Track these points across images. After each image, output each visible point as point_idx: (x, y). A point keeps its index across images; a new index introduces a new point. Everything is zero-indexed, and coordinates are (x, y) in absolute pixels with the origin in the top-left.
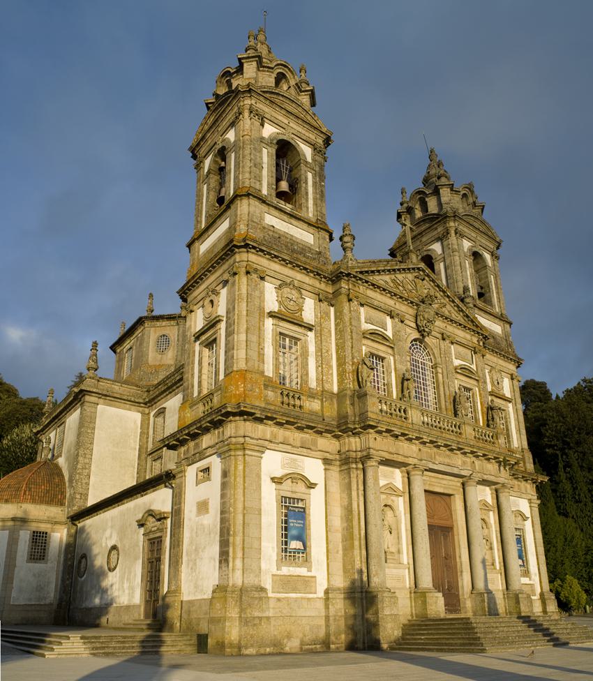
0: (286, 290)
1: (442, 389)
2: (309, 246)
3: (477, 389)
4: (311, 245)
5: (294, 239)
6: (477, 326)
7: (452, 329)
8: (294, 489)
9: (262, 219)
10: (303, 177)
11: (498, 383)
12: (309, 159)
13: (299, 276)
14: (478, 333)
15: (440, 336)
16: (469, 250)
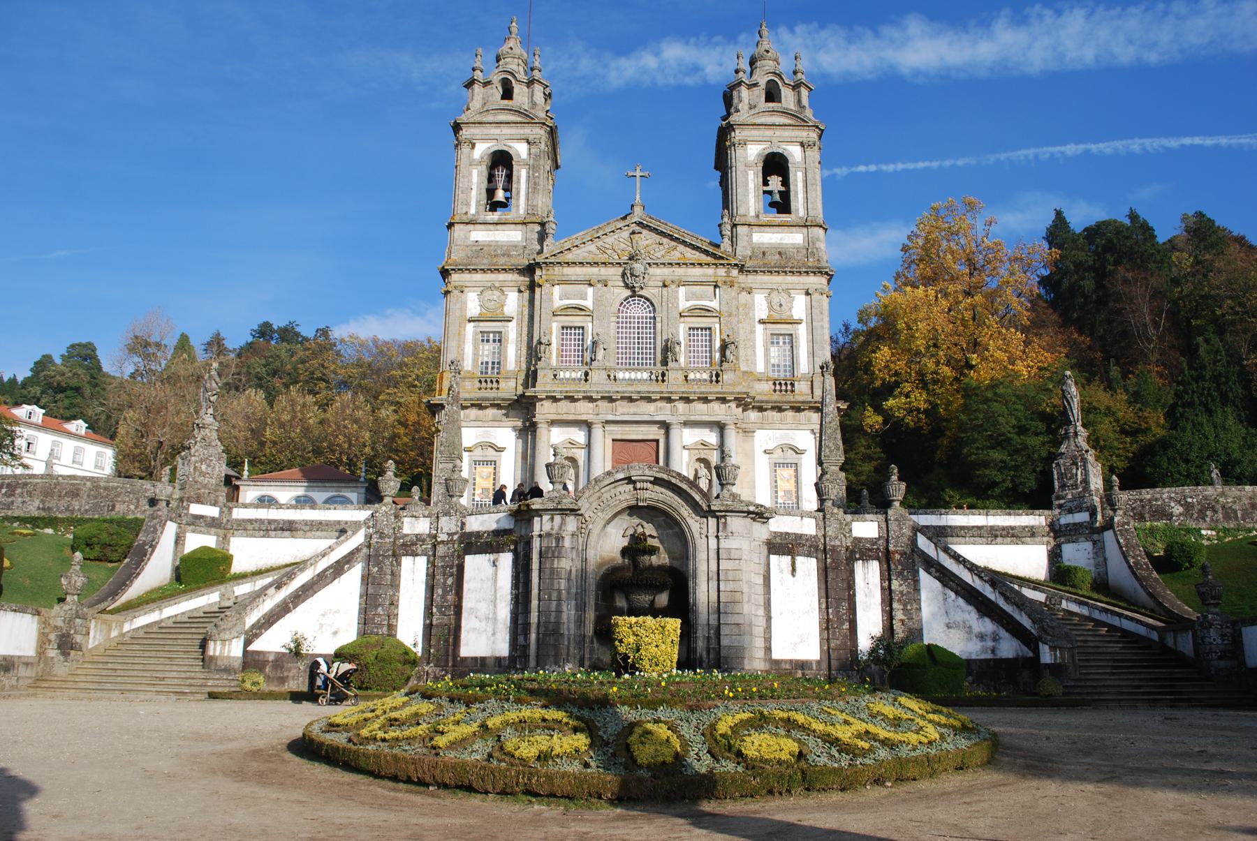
0: (488, 294)
1: (658, 338)
2: (516, 243)
3: (717, 326)
4: (518, 242)
5: (499, 244)
6: (722, 258)
7: (680, 271)
8: (485, 453)
9: (467, 238)
10: (515, 178)
11: (781, 305)
12: (524, 154)
13: (502, 277)
14: (723, 264)
15: (661, 284)
16: (759, 155)
